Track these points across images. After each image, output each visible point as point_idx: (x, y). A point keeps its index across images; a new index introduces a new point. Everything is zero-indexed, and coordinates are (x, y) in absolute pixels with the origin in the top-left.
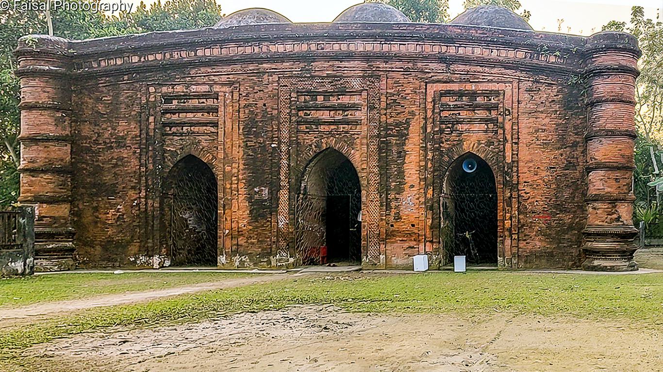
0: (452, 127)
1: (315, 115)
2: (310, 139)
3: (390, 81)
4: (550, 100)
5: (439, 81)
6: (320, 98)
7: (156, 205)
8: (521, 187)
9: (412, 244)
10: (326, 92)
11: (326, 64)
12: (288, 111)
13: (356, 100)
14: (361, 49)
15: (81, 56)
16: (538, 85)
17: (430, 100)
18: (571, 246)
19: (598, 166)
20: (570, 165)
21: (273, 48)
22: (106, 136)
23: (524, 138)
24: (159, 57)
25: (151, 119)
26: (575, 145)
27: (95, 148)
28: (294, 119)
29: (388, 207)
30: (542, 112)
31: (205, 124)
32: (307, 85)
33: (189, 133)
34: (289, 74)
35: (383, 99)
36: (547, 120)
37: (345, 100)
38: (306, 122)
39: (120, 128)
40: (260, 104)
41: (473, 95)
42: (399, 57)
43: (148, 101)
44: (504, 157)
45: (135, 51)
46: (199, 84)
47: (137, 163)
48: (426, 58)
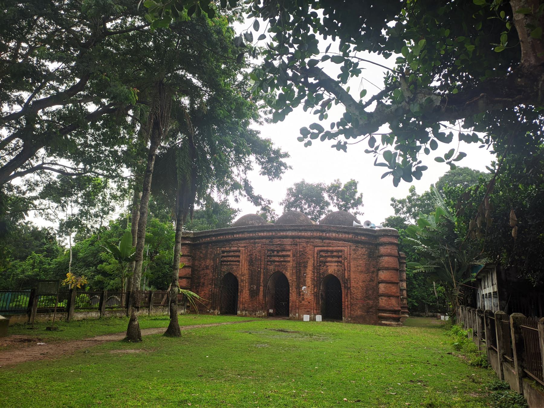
2: (271, 267)
3: (301, 246)
6: (275, 252)
8: (351, 288)
9: (309, 310)
11: (278, 240)
13: (288, 253)
19: (382, 282)
20: (371, 280)
21: (260, 234)
23: (353, 269)
24: (221, 237)
26: (373, 272)
29: (300, 295)
31: (235, 261)
33: (230, 265)
36: (361, 262)
37: (284, 253)
38: (270, 261)
41: (332, 252)
42: (304, 237)
45: (214, 236)
48: (315, 238)
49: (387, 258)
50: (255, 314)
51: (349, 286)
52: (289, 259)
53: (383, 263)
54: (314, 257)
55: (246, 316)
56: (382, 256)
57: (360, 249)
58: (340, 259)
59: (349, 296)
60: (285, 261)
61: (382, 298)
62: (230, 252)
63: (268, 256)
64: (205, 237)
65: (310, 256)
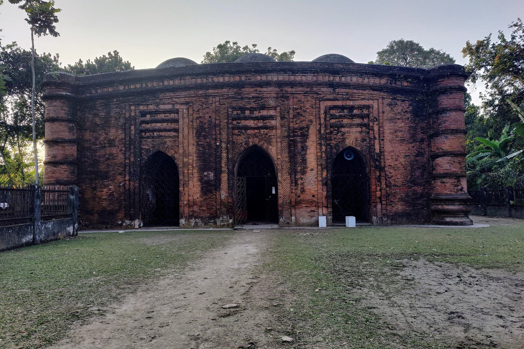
0: (338, 130)
1: (244, 123)
2: (241, 139)
3: (295, 100)
6: (247, 112)
7: (137, 185)
8: (386, 169)
9: (313, 209)
10: (252, 108)
11: (252, 90)
12: (226, 121)
13: (272, 112)
16: (396, 101)
17: (322, 112)
18: (422, 208)
19: (445, 154)
20: (420, 154)
21: (216, 79)
22: (101, 139)
23: (388, 136)
24: (138, 86)
25: (133, 128)
26: (422, 141)
27: (94, 147)
28: (230, 126)
29: (296, 184)
30: (399, 119)
31: (169, 131)
32: (241, 103)
35: (291, 111)
36: (403, 124)
37: (264, 113)
38: (238, 128)
40: (207, 116)
41: (351, 108)
42: (301, 84)
43: (130, 115)
45: (122, 83)
46: (165, 104)
48: (320, 84)
49: (454, 113)
50: (215, 223)
51: (383, 165)
53: (447, 124)
54: (320, 118)
56: (445, 110)
57: (399, 103)
58: (366, 121)
59: (383, 182)
60: (266, 128)
61: (444, 180)
62: (157, 112)
64: (102, 85)
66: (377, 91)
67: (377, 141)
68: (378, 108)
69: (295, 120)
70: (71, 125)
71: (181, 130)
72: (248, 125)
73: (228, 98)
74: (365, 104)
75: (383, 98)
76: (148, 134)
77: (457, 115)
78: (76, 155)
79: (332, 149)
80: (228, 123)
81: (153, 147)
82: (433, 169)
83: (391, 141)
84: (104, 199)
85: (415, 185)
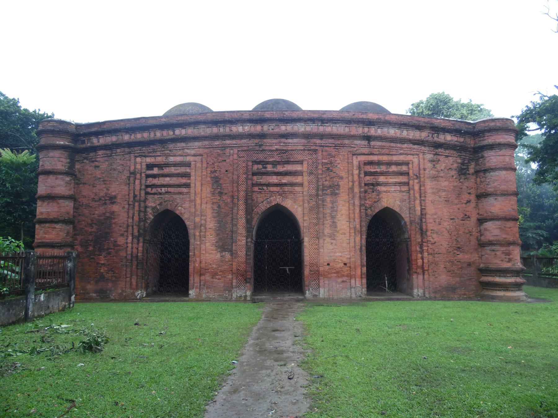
3: (324, 153)
4: (448, 168)
5: (364, 154)
7: (140, 249)
8: (429, 233)
10: (275, 161)
11: (275, 141)
13: (298, 168)
14: (303, 130)
15: (85, 135)
16: (438, 157)
20: (466, 217)
23: (430, 197)
25: (137, 182)
28: (250, 182)
31: (179, 186)
32: (261, 157)
33: (167, 192)
34: (246, 148)
35: (320, 167)
36: (446, 183)
37: (289, 168)
39: (112, 189)
41: (389, 164)
44: (415, 211)
47: (125, 215)
49: (504, 172)
52: (299, 179)
54: (353, 175)
55: (209, 300)
57: (442, 158)
62: (168, 165)
63: (254, 174)
65: (343, 174)
66: (418, 145)
67: (418, 202)
68: (419, 164)
69: (324, 176)
70: (68, 179)
71: (192, 185)
72: (271, 181)
73: (248, 151)
74: (404, 159)
75: (424, 153)
76: (154, 190)
77: (507, 174)
78: (72, 212)
79: (366, 210)
80: (247, 179)
81: (160, 204)
82: (481, 235)
83: (433, 202)
84: (103, 264)
85: (461, 252)
